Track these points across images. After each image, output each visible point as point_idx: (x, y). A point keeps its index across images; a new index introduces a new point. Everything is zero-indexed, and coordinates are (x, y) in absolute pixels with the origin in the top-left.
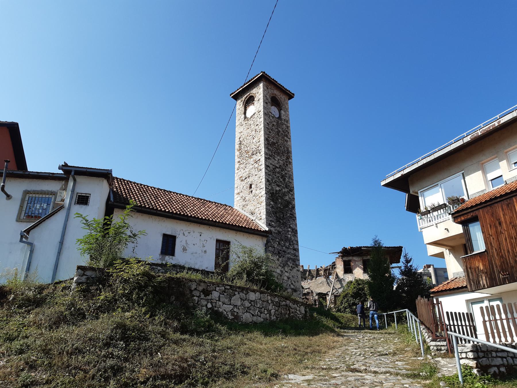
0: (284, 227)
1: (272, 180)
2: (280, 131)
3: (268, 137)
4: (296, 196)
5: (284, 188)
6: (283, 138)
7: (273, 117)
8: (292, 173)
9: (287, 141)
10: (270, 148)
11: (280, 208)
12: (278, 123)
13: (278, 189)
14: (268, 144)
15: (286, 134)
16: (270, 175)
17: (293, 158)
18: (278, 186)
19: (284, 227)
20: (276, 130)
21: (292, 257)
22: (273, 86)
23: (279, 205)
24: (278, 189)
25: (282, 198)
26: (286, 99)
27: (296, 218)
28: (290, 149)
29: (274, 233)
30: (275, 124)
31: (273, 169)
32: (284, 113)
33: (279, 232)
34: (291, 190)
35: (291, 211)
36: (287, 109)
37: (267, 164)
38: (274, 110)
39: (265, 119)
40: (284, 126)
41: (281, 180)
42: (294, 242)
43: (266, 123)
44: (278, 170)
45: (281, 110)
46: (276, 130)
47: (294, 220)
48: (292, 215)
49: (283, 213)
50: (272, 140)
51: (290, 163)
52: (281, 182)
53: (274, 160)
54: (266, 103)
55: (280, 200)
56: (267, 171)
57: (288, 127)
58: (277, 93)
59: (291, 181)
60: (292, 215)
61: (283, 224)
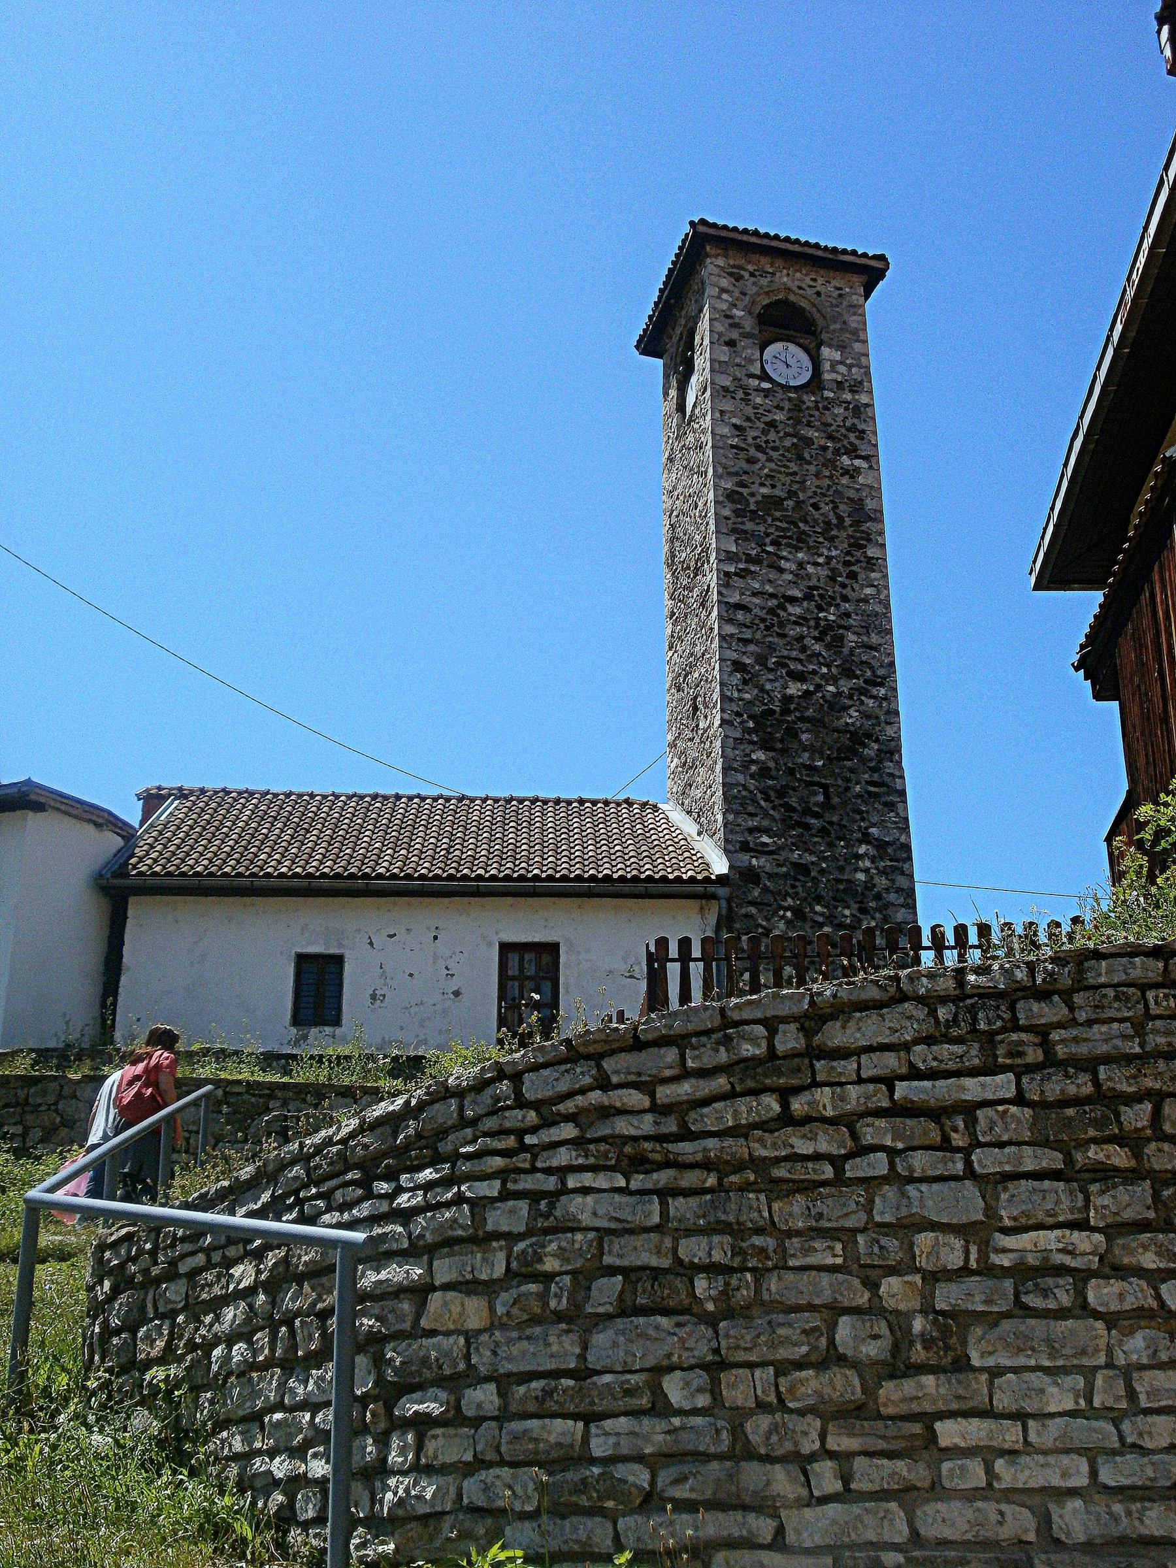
1: (761, 660)
2: (809, 442)
6: (831, 464)
7: (767, 393)
8: (887, 606)
9: (853, 473)
10: (749, 526)
11: (809, 768)
12: (797, 407)
13: (794, 689)
15: (854, 438)
16: (746, 642)
18: (799, 677)
19: (831, 845)
20: (788, 442)
24: (794, 689)
25: (817, 724)
26: (852, 286)
27: (902, 793)
28: (870, 504)
29: (770, 876)
30: (779, 416)
31: (771, 611)
32: (837, 356)
34: (878, 678)
35: (874, 770)
36: (859, 334)
37: (735, 598)
38: (788, 363)
41: (817, 647)
42: (892, 897)
43: (726, 430)
44: (795, 610)
45: (820, 344)
46: (788, 442)
47: (891, 806)
50: (764, 490)
51: (876, 564)
53: (773, 575)
54: (731, 343)
55: (804, 737)
56: (730, 629)
57: (862, 411)
58: (791, 281)
59: (875, 639)
61: (824, 832)
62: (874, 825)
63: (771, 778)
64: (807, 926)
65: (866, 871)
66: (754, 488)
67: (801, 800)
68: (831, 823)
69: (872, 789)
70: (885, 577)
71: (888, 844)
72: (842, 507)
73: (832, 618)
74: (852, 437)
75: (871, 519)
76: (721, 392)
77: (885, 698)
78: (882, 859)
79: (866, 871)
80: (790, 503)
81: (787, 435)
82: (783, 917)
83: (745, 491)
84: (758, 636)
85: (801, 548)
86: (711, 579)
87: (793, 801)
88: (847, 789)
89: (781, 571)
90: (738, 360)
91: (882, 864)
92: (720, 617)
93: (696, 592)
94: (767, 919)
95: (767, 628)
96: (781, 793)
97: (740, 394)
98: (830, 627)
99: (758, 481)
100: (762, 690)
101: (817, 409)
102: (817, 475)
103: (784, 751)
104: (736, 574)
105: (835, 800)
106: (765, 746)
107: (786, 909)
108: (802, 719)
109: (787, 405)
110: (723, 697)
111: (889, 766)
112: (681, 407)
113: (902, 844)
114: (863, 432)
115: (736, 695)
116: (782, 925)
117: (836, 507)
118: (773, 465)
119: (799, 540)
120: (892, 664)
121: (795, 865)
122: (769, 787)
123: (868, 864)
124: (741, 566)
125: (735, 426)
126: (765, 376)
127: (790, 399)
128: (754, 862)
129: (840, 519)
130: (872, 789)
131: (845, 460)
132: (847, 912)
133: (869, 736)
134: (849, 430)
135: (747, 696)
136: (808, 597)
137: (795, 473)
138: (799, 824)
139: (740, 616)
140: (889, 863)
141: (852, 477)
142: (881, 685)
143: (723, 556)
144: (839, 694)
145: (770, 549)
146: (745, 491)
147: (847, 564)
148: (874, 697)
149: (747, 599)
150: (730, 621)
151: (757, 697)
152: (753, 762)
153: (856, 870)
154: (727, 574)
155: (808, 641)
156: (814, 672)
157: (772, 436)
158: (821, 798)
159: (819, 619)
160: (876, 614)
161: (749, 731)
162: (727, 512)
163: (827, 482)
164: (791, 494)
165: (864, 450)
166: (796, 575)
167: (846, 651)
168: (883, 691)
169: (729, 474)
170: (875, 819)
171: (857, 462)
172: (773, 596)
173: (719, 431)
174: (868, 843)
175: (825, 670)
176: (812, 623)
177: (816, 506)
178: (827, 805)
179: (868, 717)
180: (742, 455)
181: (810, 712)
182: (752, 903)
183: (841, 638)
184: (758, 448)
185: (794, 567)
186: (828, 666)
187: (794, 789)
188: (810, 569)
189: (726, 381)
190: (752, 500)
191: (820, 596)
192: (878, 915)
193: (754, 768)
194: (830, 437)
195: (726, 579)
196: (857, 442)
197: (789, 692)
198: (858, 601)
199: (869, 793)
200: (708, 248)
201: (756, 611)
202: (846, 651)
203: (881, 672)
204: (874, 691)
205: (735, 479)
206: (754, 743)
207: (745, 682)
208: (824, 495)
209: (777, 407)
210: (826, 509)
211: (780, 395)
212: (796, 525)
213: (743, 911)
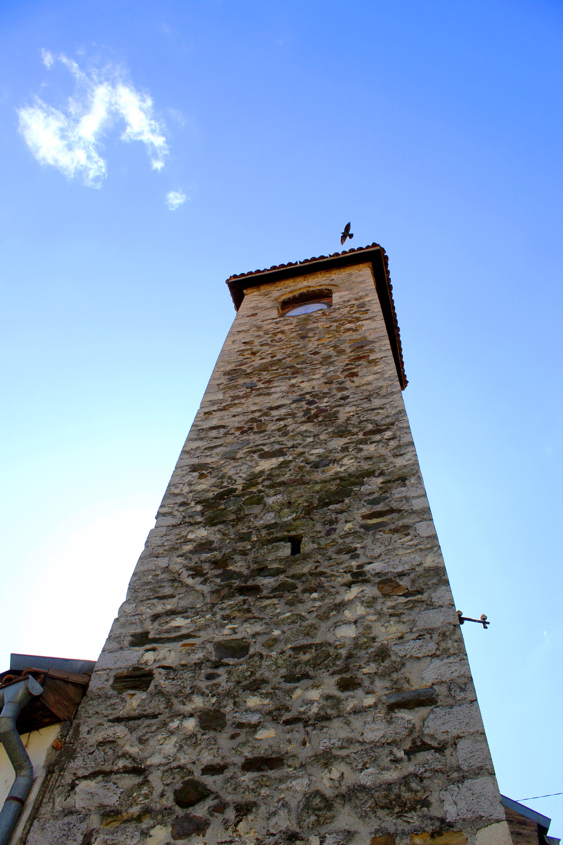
21: (366, 778)
48: (392, 511)
60: (392, 511)
91: (389, 603)
94: (142, 741)
113: (428, 570)
123: (360, 610)
132: (314, 694)
138: (242, 591)
140: (403, 600)
192: (380, 685)
199: (367, 528)
200: (245, 291)
213: (100, 736)
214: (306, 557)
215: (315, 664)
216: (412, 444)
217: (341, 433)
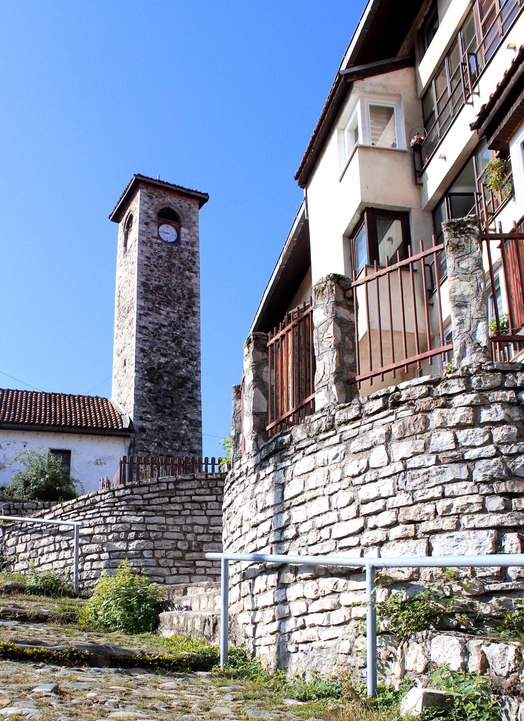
0: (173, 420)
1: (151, 348)
2: (174, 265)
3: (147, 280)
4: (203, 368)
5: (176, 357)
6: (181, 274)
7: (159, 245)
8: (199, 331)
10: (150, 296)
11: (166, 390)
12: (170, 251)
13: (163, 360)
14: (146, 291)
15: (190, 265)
16: (146, 341)
17: (201, 305)
19: (173, 420)
22: (162, 193)
23: (165, 386)
24: (163, 360)
25: (169, 374)
26: (194, 205)
27: (200, 402)
28: (195, 291)
30: (164, 254)
31: (156, 330)
33: (161, 428)
34: (194, 358)
35: (190, 392)
37: (143, 324)
39: (141, 252)
40: (186, 253)
41: (172, 345)
43: (143, 258)
44: (165, 330)
46: (166, 264)
47: (196, 406)
49: (172, 398)
50: (156, 283)
52: (171, 348)
53: (157, 316)
55: (166, 379)
56: (140, 336)
59: (194, 343)
61: (170, 415)
62: (189, 413)
63: (152, 393)
64: (162, 449)
65: (184, 430)
66: (152, 281)
67: (164, 402)
68: (173, 411)
69: (189, 400)
70: (199, 319)
71: (194, 420)
72: (185, 291)
73: (178, 334)
74: (191, 264)
75: (195, 297)
76: (142, 243)
77: (196, 366)
78: (191, 425)
79: (184, 430)
80: (165, 289)
81: (166, 261)
82: (153, 445)
83: (149, 283)
84: (151, 339)
85: (167, 306)
86: (133, 315)
87: (159, 402)
88: (180, 399)
89: (161, 314)
90: (149, 231)
92: (137, 331)
93: (128, 319)
95: (154, 336)
96: (156, 399)
97: (149, 244)
98: (177, 337)
99: (154, 279)
100: (151, 360)
101: (178, 252)
102: (176, 278)
103: (158, 383)
104: (144, 315)
105: (175, 403)
106: (151, 381)
107: (155, 442)
108: (165, 372)
109: (166, 250)
110: (137, 362)
111: (195, 392)
112: (125, 245)
114: (195, 262)
115: (141, 361)
116: (153, 448)
117: (182, 291)
118: (160, 273)
119: (168, 303)
120: (199, 353)
121: (159, 426)
122: (152, 397)
123: (185, 427)
124: (146, 311)
125: (147, 257)
126: (159, 238)
127: (168, 248)
128: (144, 424)
129: (184, 296)
130: (189, 400)
131: (187, 273)
133: (189, 379)
134: (189, 261)
135: (145, 362)
136: (170, 325)
137: (168, 277)
139: (144, 331)
141: (189, 280)
142: (195, 360)
143: (139, 307)
144: (179, 363)
145: (157, 306)
146: (149, 283)
147: (185, 313)
148: (192, 365)
149: (147, 325)
150: (140, 333)
151: (148, 363)
152: (146, 387)
153: (182, 429)
154: (140, 314)
155: (169, 342)
156: (170, 354)
157: (160, 261)
158: (170, 402)
159: (173, 334)
160: (195, 334)
161: (145, 375)
162: (142, 290)
163: (180, 281)
164: (166, 285)
165: (195, 269)
166: (166, 317)
167: (183, 346)
168: (195, 363)
169: (143, 275)
170: (189, 411)
171: (192, 274)
172: (156, 324)
173: (140, 258)
174: (186, 419)
175: (174, 353)
176: (171, 335)
177: (175, 290)
178: (172, 405)
179: (189, 372)
180: (148, 268)
181: (168, 369)
182: (142, 439)
183: (181, 342)
184: (155, 266)
185: (165, 313)
186: (176, 352)
187: (161, 398)
188: (171, 314)
189: (144, 239)
190: (151, 286)
191: (175, 325)
193: (146, 389)
194: (182, 263)
195: (140, 316)
196: (192, 266)
197: (160, 361)
198: (189, 328)
201: (150, 329)
202: (183, 346)
203: (195, 356)
204: (192, 363)
205: (145, 278)
206: (146, 380)
207: (145, 356)
208: (178, 286)
209: (164, 251)
210: (179, 291)
211: (164, 246)
212: (167, 297)
214: (174, 406)
215: (177, 437)
216: (200, 372)
217: (183, 355)
